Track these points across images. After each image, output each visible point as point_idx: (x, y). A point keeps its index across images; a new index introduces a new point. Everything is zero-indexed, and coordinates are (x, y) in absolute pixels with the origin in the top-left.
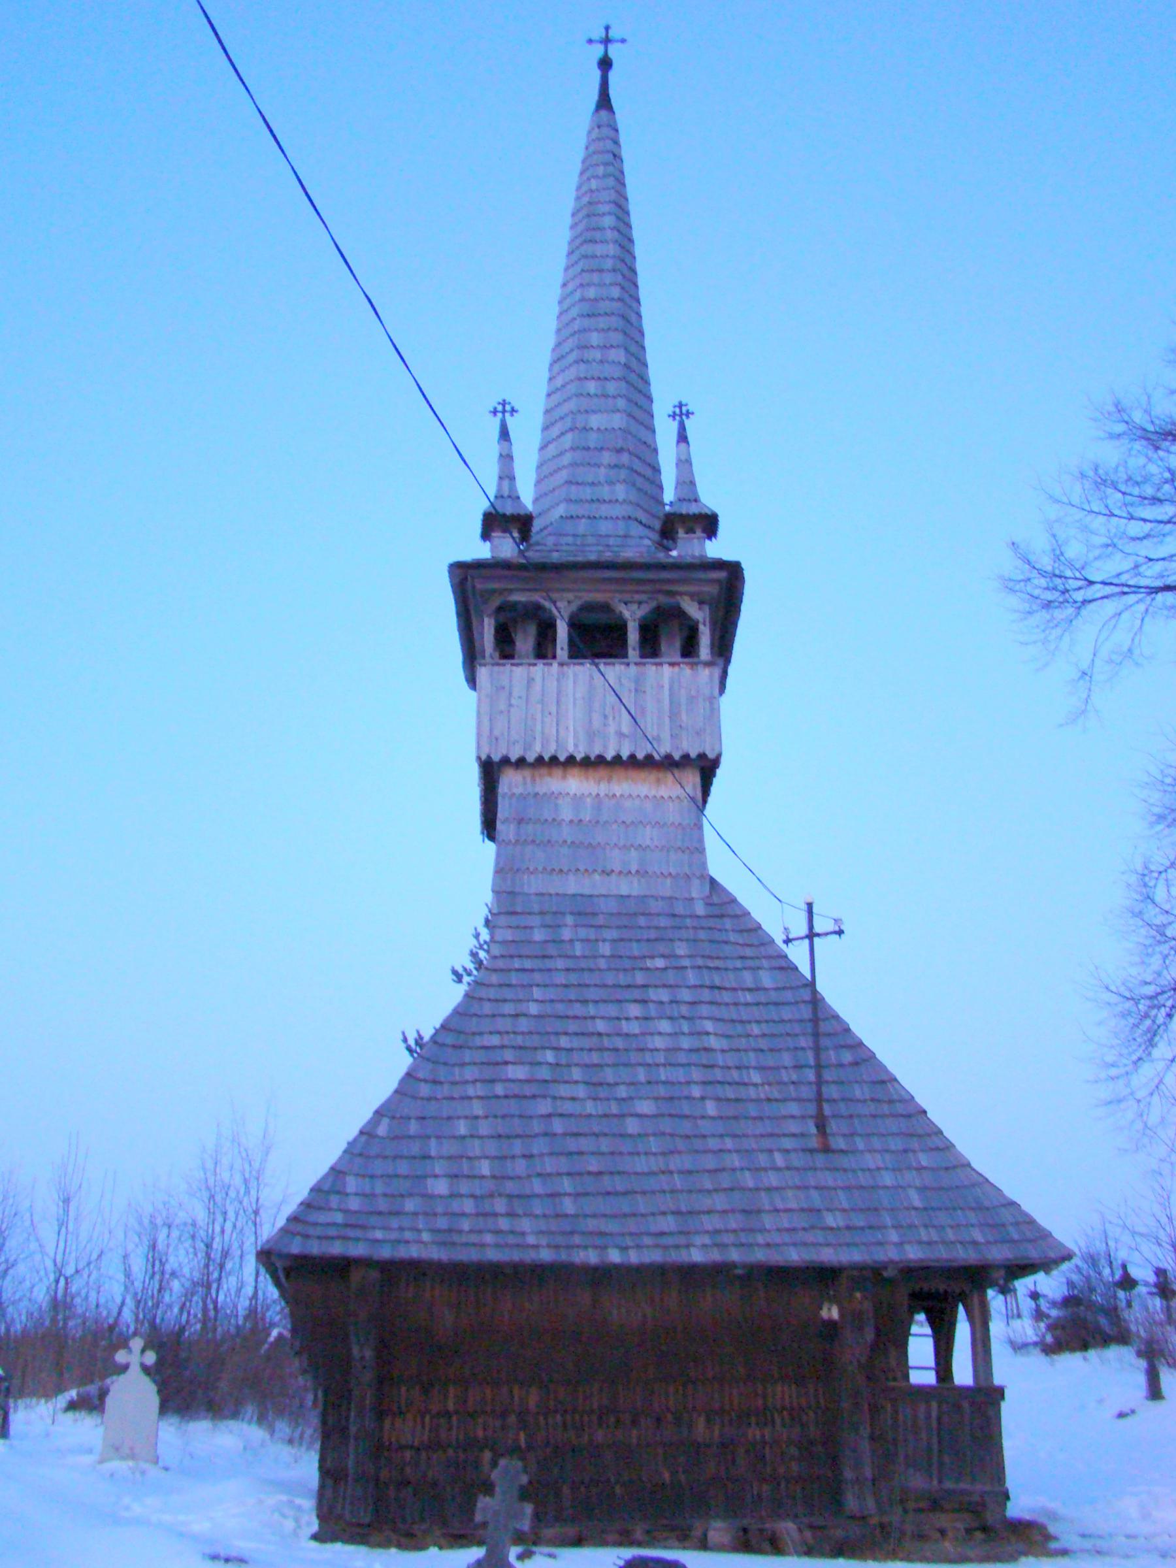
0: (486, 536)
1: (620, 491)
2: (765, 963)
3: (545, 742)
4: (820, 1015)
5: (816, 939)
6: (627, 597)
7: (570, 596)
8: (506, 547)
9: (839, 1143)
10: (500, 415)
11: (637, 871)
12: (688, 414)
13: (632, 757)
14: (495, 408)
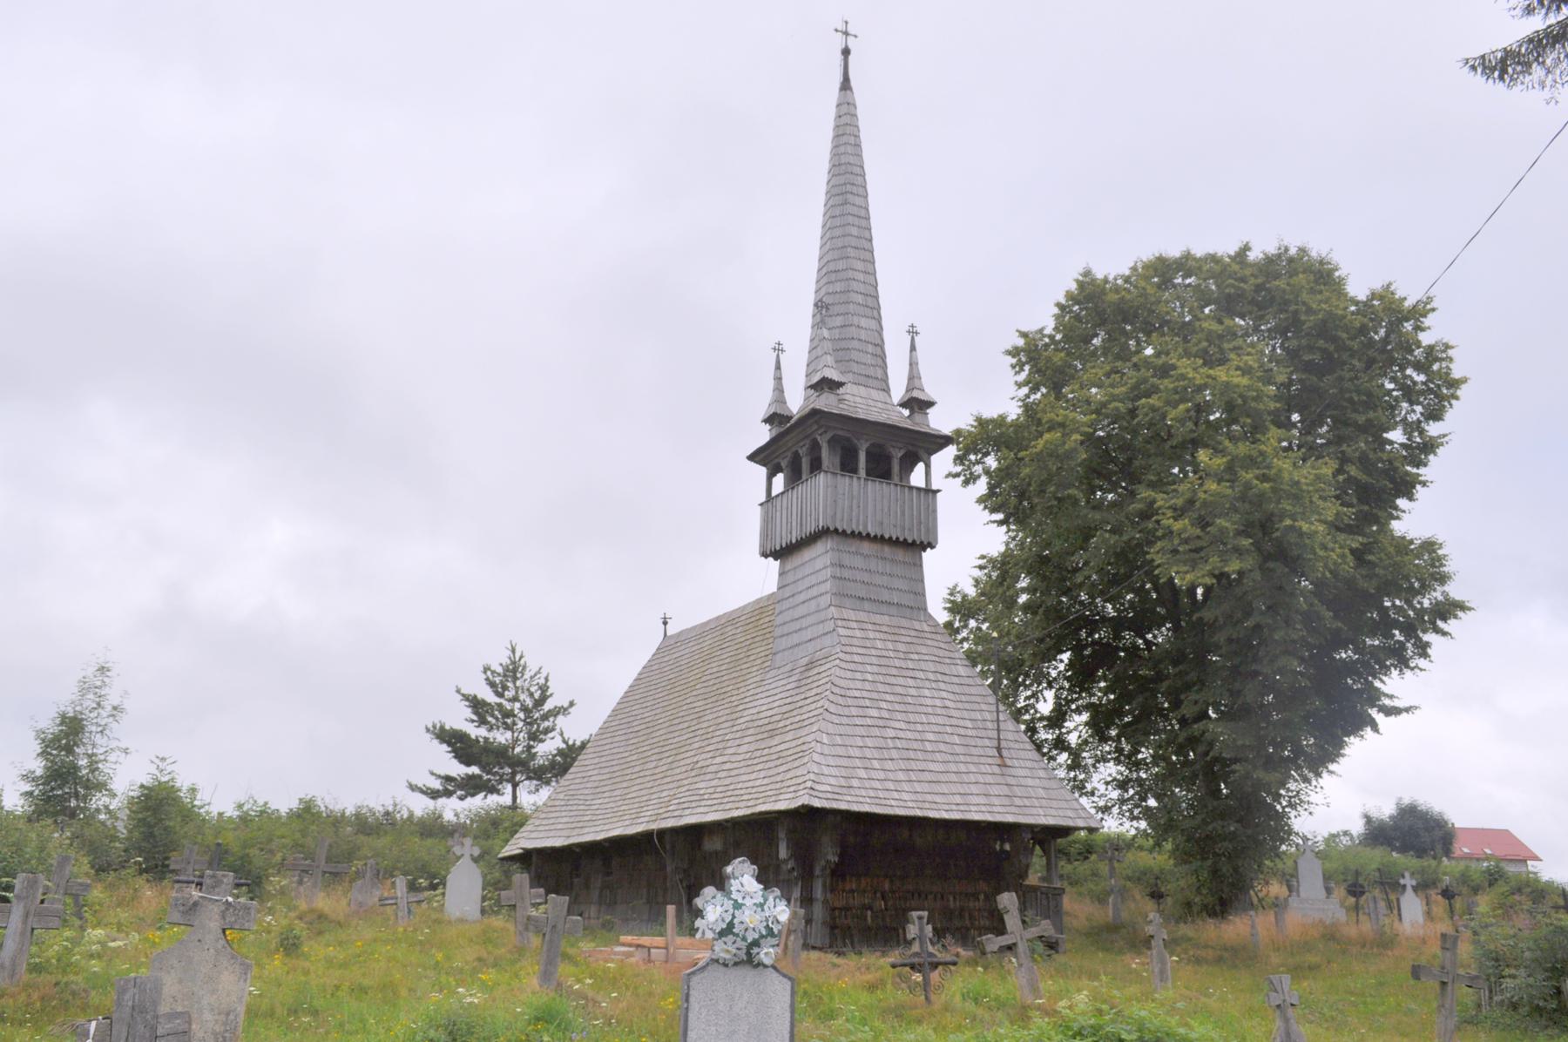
6: (894, 444)
9: (1009, 762)
13: (897, 538)
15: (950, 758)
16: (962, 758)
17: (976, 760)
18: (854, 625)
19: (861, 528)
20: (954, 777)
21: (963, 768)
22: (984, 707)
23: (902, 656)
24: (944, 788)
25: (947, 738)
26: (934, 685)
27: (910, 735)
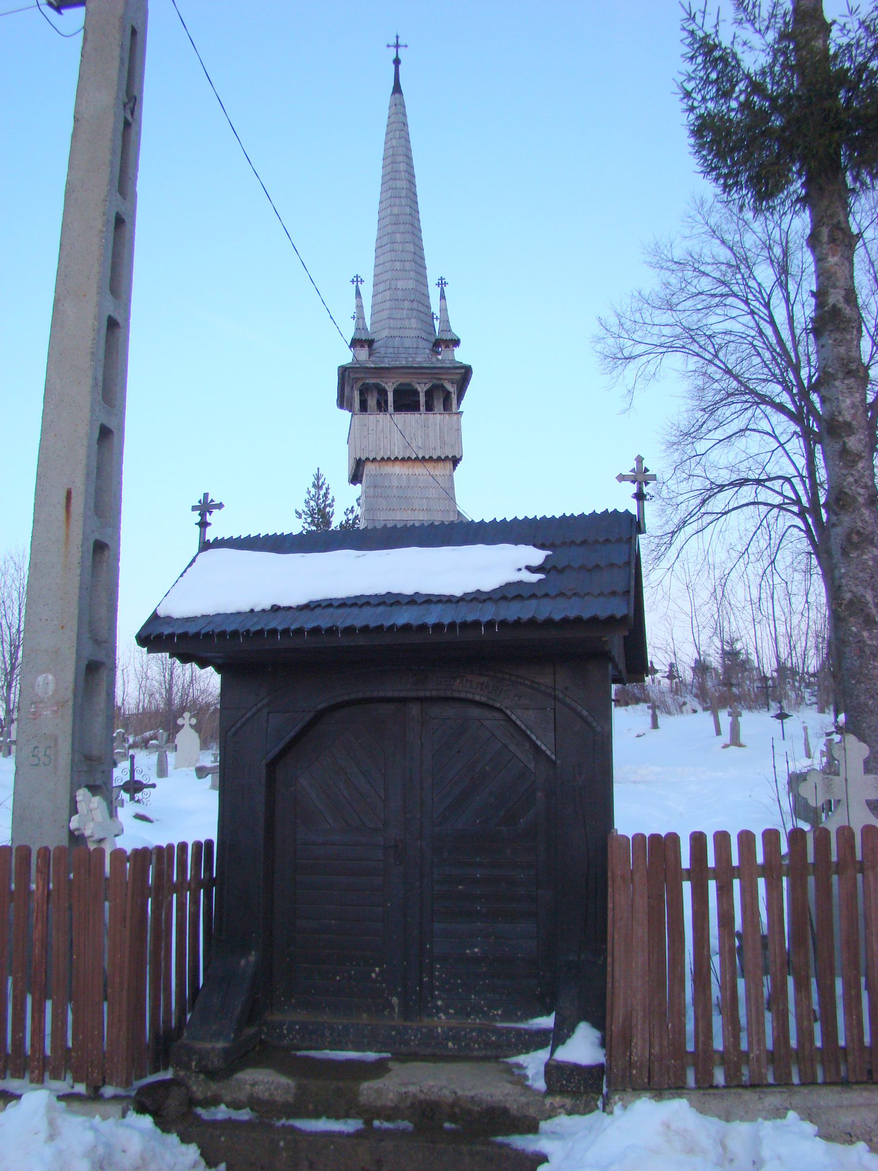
1: (414, 323)
6: (419, 381)
7: (394, 380)
10: (355, 283)
12: (445, 284)
13: (423, 457)
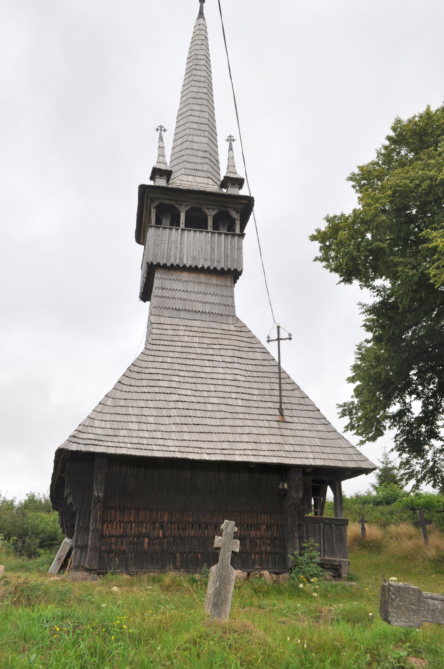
0: (152, 178)
2: (258, 350)
3: (175, 259)
4: (281, 371)
5: (281, 341)
6: (209, 207)
8: (161, 182)
9: (288, 419)
10: (159, 131)
11: (209, 312)
13: (209, 268)
14: (158, 128)
15: (229, 415)
16: (241, 416)
17: (255, 417)
18: (169, 327)
19: (178, 262)
20: (228, 430)
21: (239, 422)
22: (273, 380)
23: (205, 346)
24: (214, 437)
25: (230, 401)
26: (228, 365)
27: (193, 399)
